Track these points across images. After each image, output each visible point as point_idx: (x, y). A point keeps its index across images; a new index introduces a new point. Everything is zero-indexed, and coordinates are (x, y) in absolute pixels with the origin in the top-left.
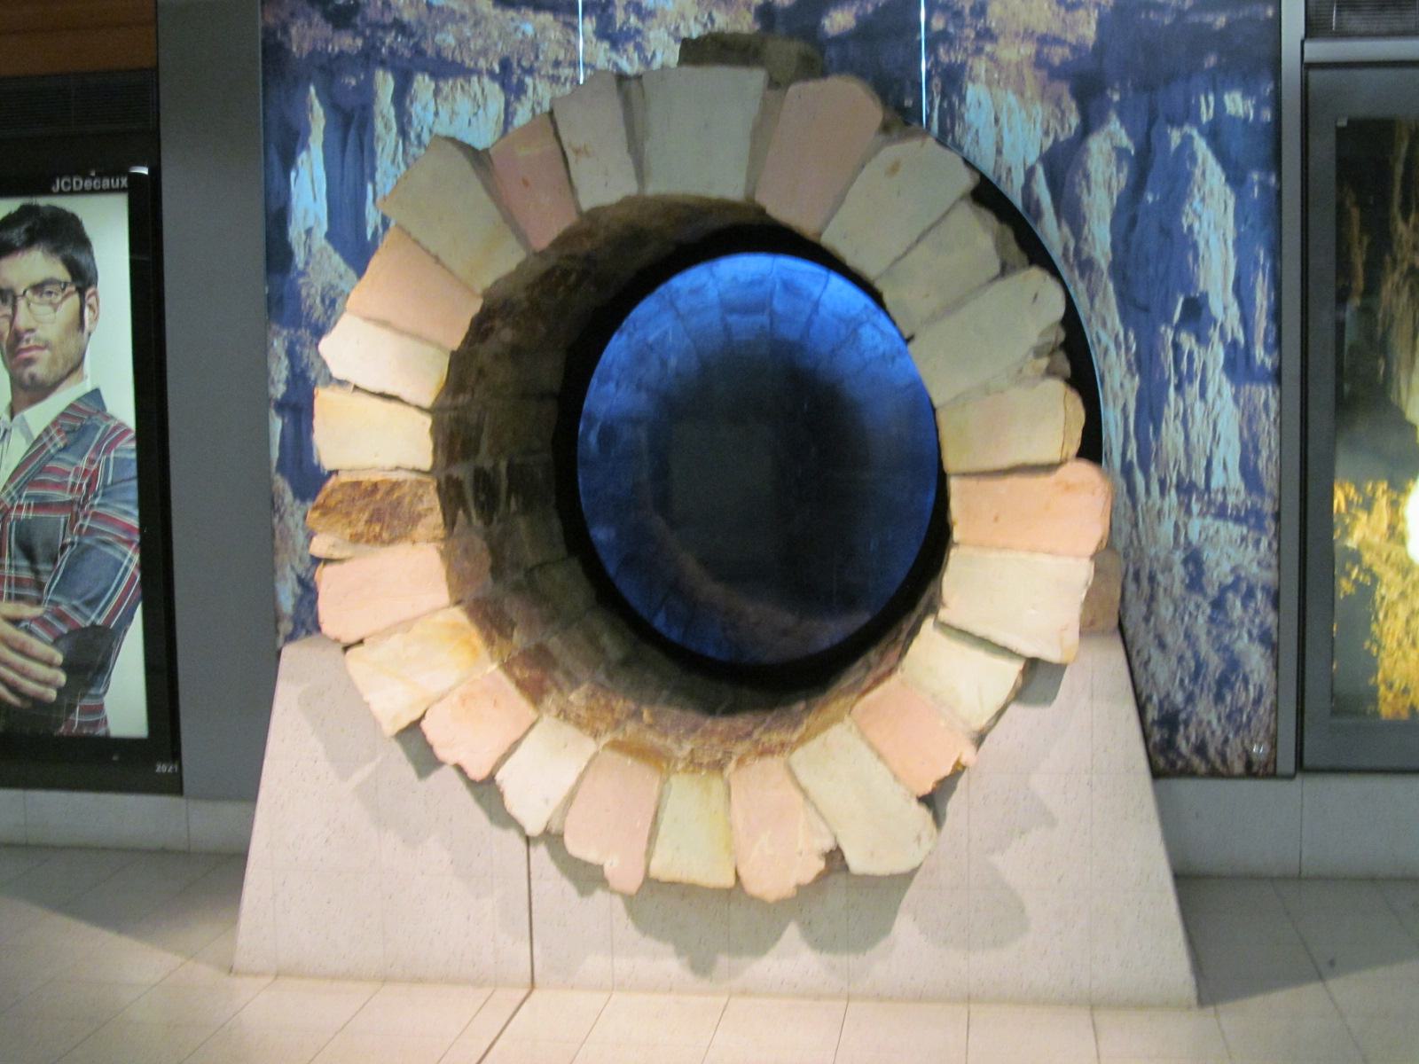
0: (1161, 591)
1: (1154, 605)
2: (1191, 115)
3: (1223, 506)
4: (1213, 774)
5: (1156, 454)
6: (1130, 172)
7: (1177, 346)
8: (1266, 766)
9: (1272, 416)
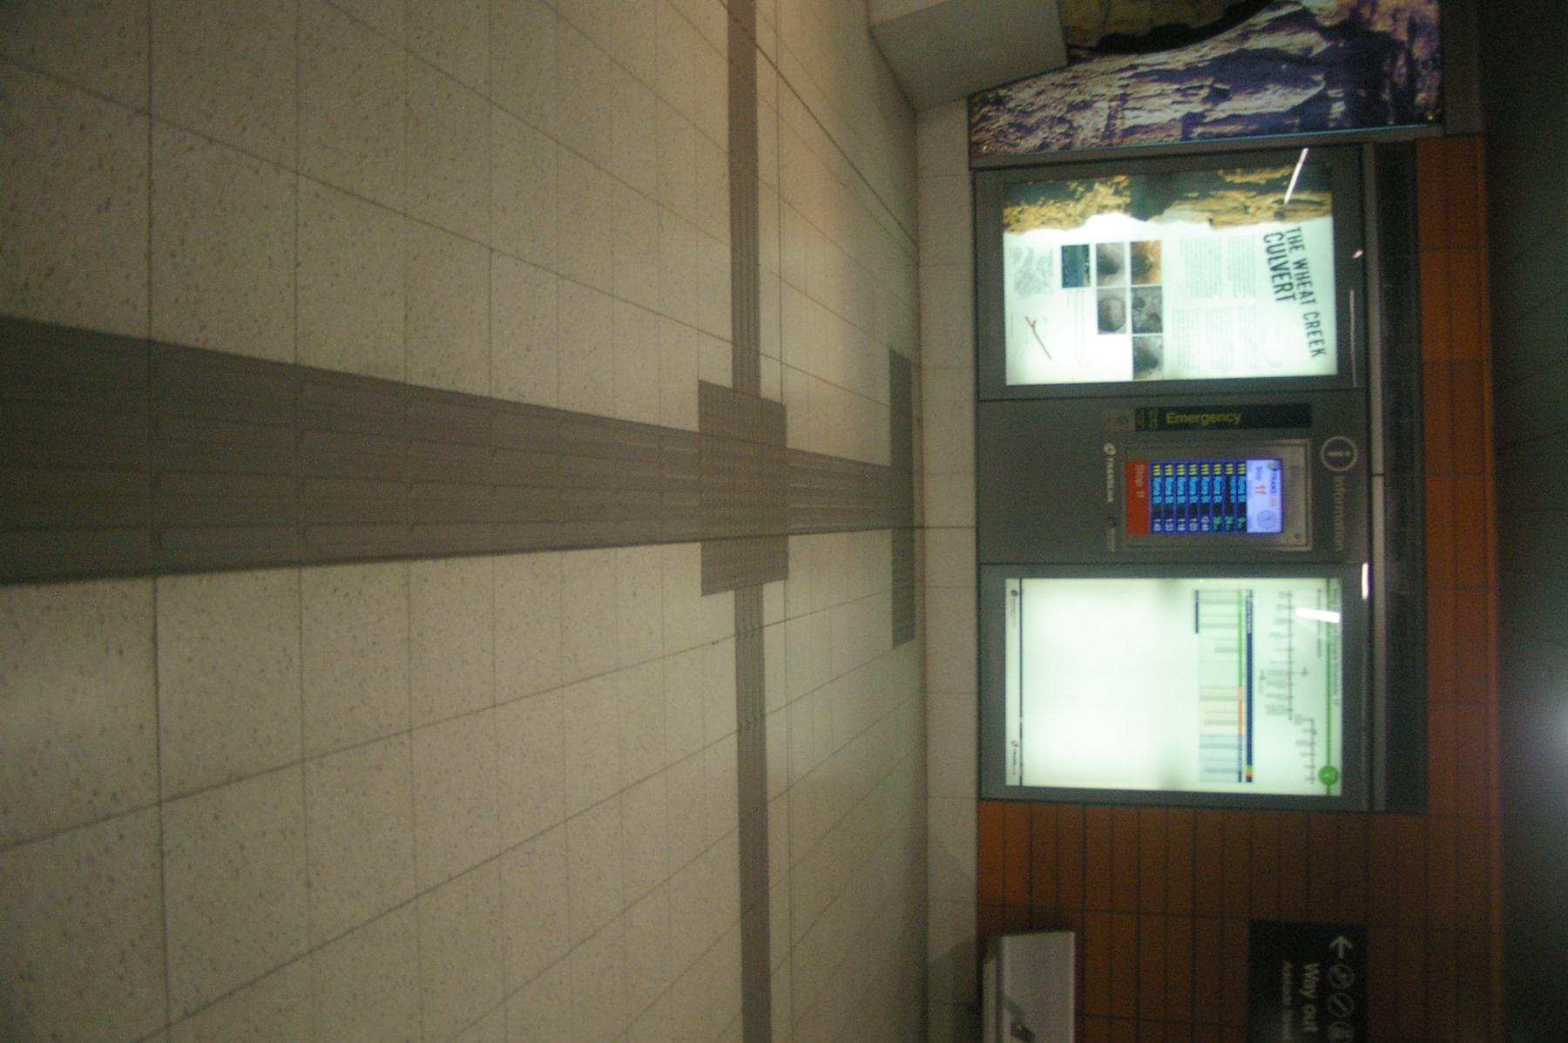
2: (1331, 84)
4: (971, 126)
7: (1201, 87)
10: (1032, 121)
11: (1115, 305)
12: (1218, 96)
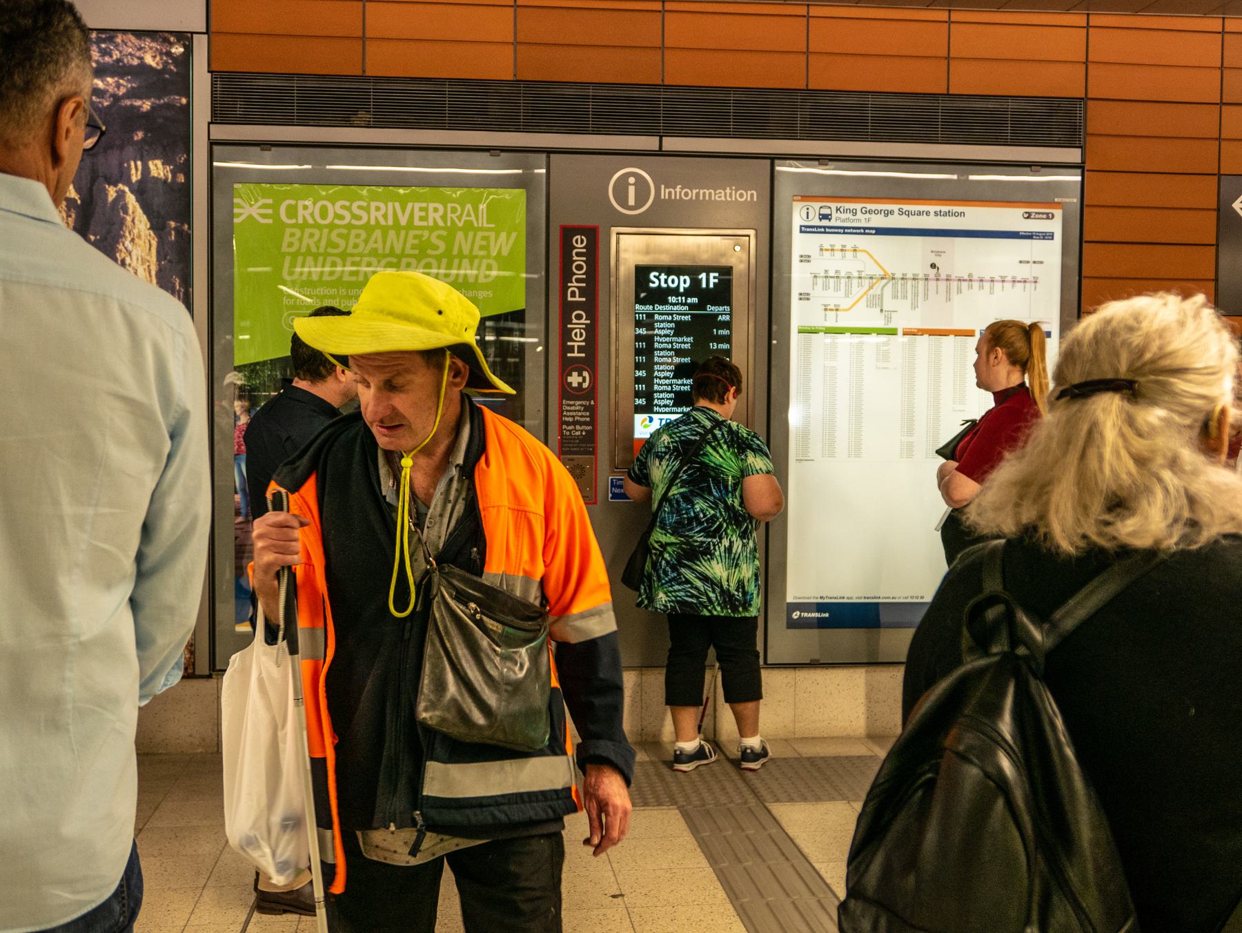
2: (124, 177)
6: (77, 217)
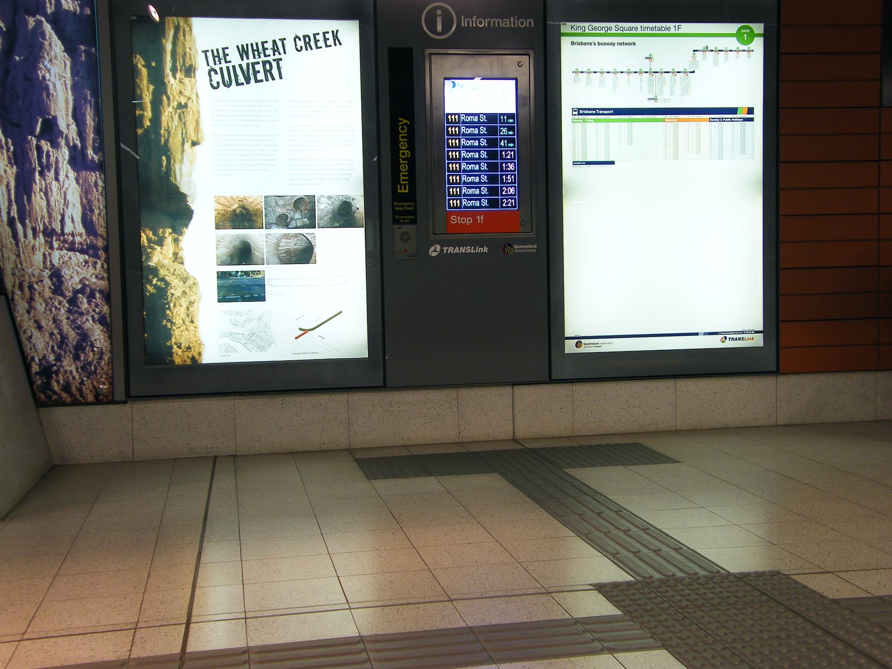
0: (37, 295)
1: (33, 304)
3: (73, 243)
4: (75, 403)
5: (30, 212)
7: (39, 148)
8: (107, 396)
9: (100, 189)
10: (72, 335)
11: (285, 245)
12: (51, 130)
